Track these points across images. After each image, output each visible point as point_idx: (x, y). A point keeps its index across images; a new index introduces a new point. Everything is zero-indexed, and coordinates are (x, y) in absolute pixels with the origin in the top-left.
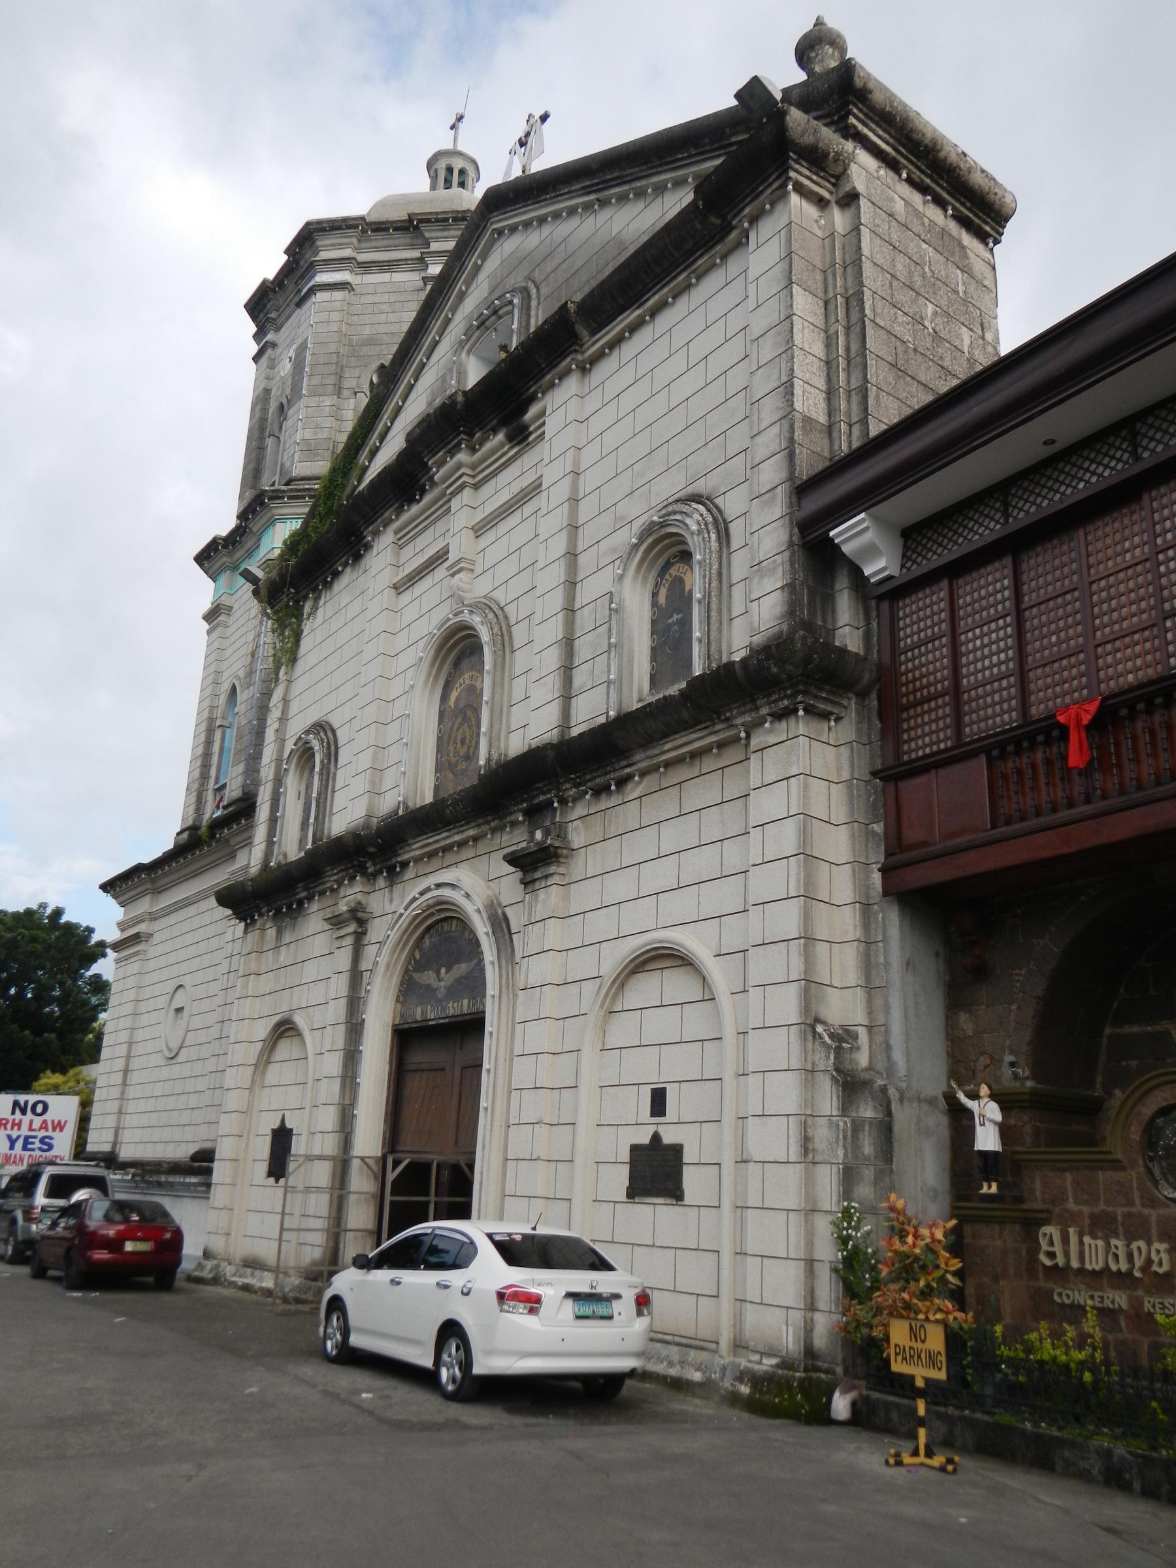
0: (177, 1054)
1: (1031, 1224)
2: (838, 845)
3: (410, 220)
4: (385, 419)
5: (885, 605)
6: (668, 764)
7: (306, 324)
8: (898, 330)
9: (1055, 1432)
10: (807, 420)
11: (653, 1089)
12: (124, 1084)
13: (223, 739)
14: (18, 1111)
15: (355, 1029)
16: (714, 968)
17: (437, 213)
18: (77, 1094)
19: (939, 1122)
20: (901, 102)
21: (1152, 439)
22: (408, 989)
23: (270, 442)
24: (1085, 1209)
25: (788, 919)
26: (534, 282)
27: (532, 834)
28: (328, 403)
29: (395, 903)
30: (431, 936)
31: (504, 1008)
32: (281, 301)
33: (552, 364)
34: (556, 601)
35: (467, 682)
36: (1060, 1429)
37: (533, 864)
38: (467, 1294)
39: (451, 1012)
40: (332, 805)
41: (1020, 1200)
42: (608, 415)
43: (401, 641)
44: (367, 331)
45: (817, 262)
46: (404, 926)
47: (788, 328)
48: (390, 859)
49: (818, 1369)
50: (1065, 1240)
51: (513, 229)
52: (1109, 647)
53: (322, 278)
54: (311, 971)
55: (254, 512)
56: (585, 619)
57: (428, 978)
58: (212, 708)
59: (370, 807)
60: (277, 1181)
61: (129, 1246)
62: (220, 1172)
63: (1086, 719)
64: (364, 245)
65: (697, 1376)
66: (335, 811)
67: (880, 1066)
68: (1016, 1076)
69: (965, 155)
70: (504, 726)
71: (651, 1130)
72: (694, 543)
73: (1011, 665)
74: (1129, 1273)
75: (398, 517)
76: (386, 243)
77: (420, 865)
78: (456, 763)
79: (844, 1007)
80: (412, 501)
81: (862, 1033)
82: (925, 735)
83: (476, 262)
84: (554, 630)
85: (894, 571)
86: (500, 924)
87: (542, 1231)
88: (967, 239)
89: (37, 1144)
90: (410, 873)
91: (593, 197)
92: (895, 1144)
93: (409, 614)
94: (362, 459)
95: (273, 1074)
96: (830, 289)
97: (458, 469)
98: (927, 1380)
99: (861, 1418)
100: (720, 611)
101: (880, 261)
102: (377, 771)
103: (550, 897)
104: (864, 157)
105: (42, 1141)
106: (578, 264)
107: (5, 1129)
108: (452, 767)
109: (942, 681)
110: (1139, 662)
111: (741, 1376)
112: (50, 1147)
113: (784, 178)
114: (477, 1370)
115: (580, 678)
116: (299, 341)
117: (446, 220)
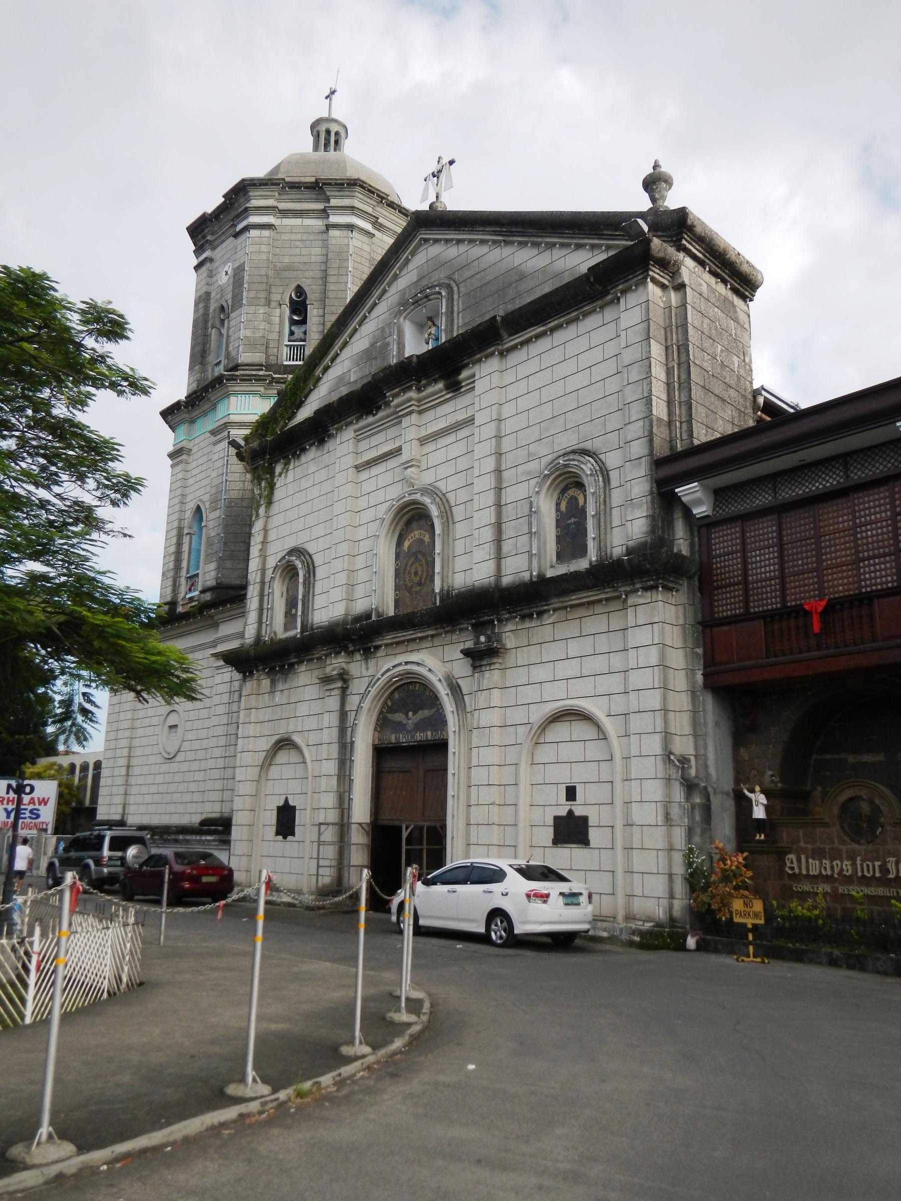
0: (175, 756)
1: (781, 854)
2: (678, 659)
3: (317, 182)
4: (336, 348)
5: (704, 531)
6: (572, 606)
7: (243, 252)
8: (705, 365)
9: (804, 947)
10: (659, 419)
11: (567, 787)
12: (128, 775)
13: (190, 543)
14: (11, 792)
15: (345, 748)
16: (608, 724)
17: (336, 179)
18: (52, 778)
19: (730, 804)
20: (711, 230)
21: (855, 468)
22: (383, 723)
23: (214, 333)
24: (810, 847)
25: (654, 700)
26: (454, 281)
27: (478, 638)
28: (261, 311)
29: (370, 670)
31: (462, 738)
32: (216, 228)
33: (481, 349)
34: (489, 499)
36: (806, 945)
38: (507, 894)
39: (419, 738)
41: (775, 842)
42: (521, 387)
43: (363, 503)
44: (287, 260)
45: (662, 324)
47: (647, 364)
49: (676, 927)
50: (799, 861)
51: (436, 241)
52: (830, 571)
53: (254, 219)
54: (302, 709)
55: (213, 387)
56: (509, 512)
57: (399, 717)
58: (180, 520)
59: (347, 609)
60: (285, 837)
61: (205, 879)
62: (236, 833)
63: (820, 609)
64: (282, 197)
65: (605, 934)
67: (702, 776)
68: (772, 781)
69: (739, 254)
70: (451, 570)
71: (569, 807)
72: (586, 481)
73: (777, 573)
74: (832, 876)
75: (357, 421)
76: (298, 196)
77: (389, 648)
78: (412, 587)
79: (683, 746)
80: (369, 412)
81: (692, 758)
82: (727, 604)
83: (407, 257)
84: (489, 516)
85: (709, 513)
86: (455, 690)
87: (531, 863)
88: (737, 301)
89: (28, 814)
90: (382, 652)
91: (500, 238)
92: (713, 816)
93: (369, 486)
94: (318, 372)
95: (274, 771)
96: (669, 340)
98: (753, 925)
99: (701, 947)
100: (605, 522)
101: (696, 324)
102: (351, 586)
103: (491, 676)
104: (689, 262)
105: (31, 812)
106: (489, 278)
107: (2, 804)
108: (409, 589)
109: (738, 576)
110: (845, 581)
111: (634, 932)
112: (38, 816)
113: (645, 274)
114: (516, 932)
115: (507, 547)
116: (237, 264)
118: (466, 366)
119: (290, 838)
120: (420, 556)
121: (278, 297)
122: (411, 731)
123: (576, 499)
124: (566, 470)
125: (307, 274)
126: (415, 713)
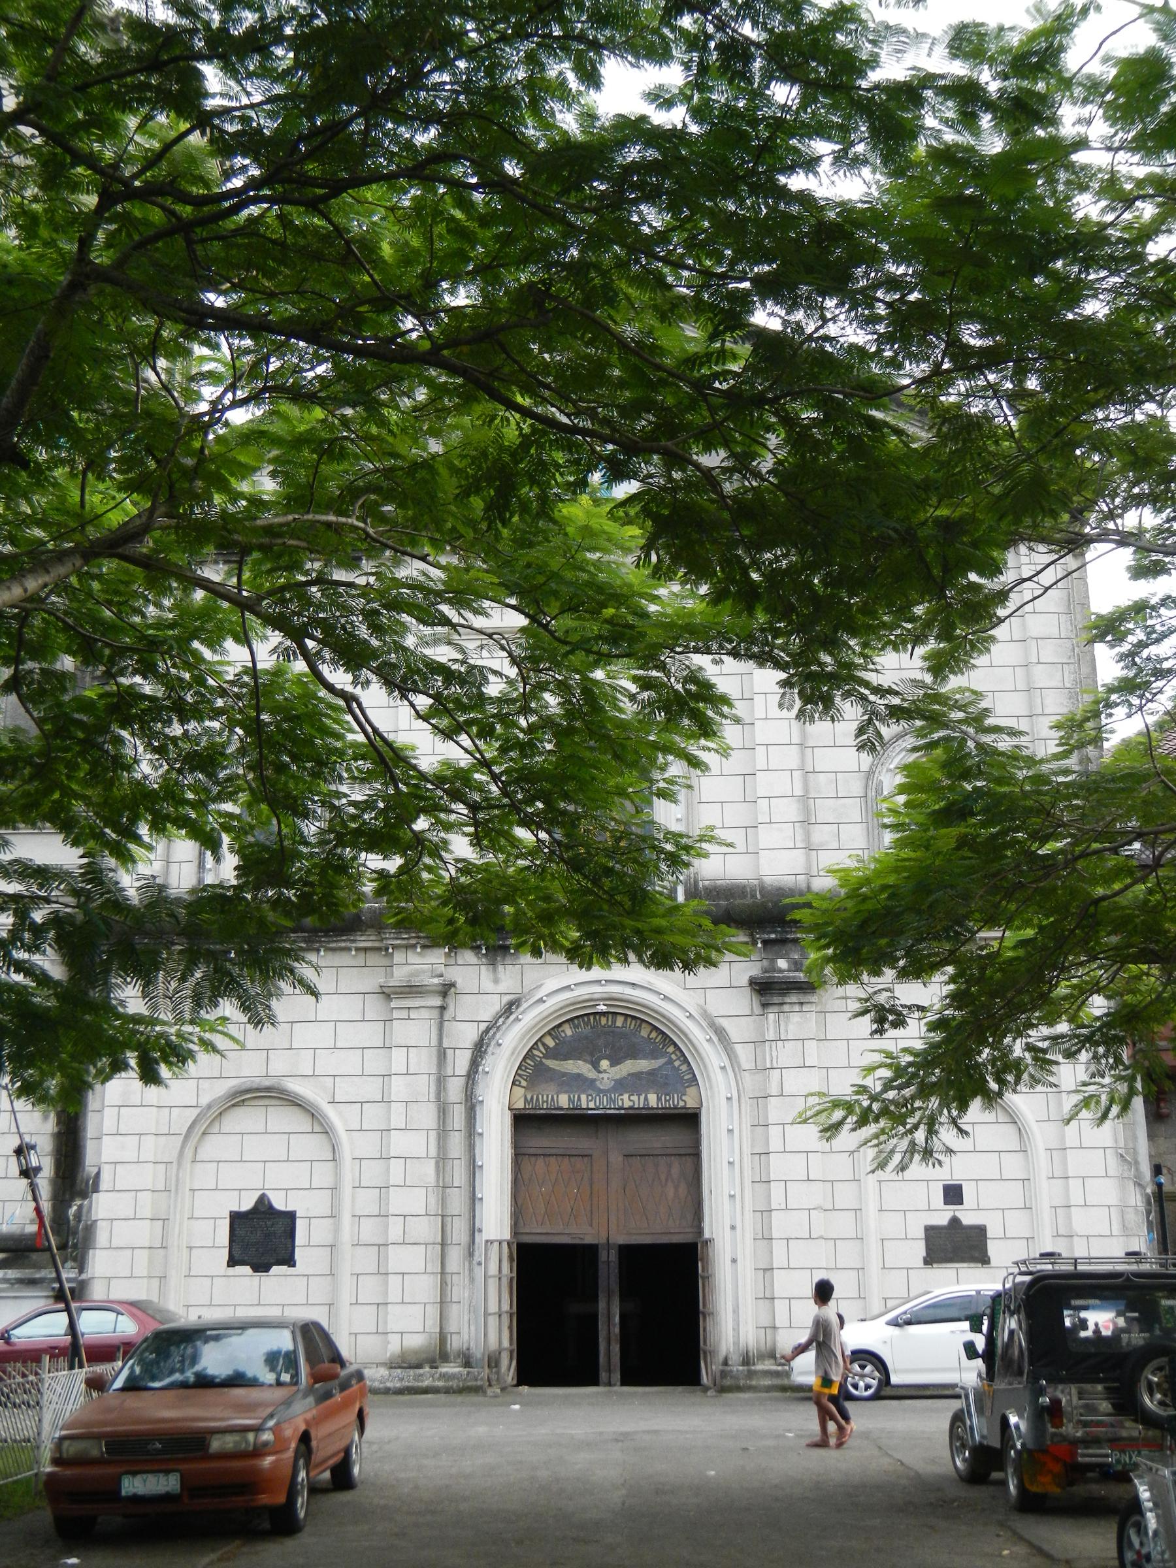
30: (576, 1027)
39: (627, 1104)
48: (505, 939)
95: (213, 1147)
119: (275, 1269)
122: (605, 1092)
126: (614, 1064)
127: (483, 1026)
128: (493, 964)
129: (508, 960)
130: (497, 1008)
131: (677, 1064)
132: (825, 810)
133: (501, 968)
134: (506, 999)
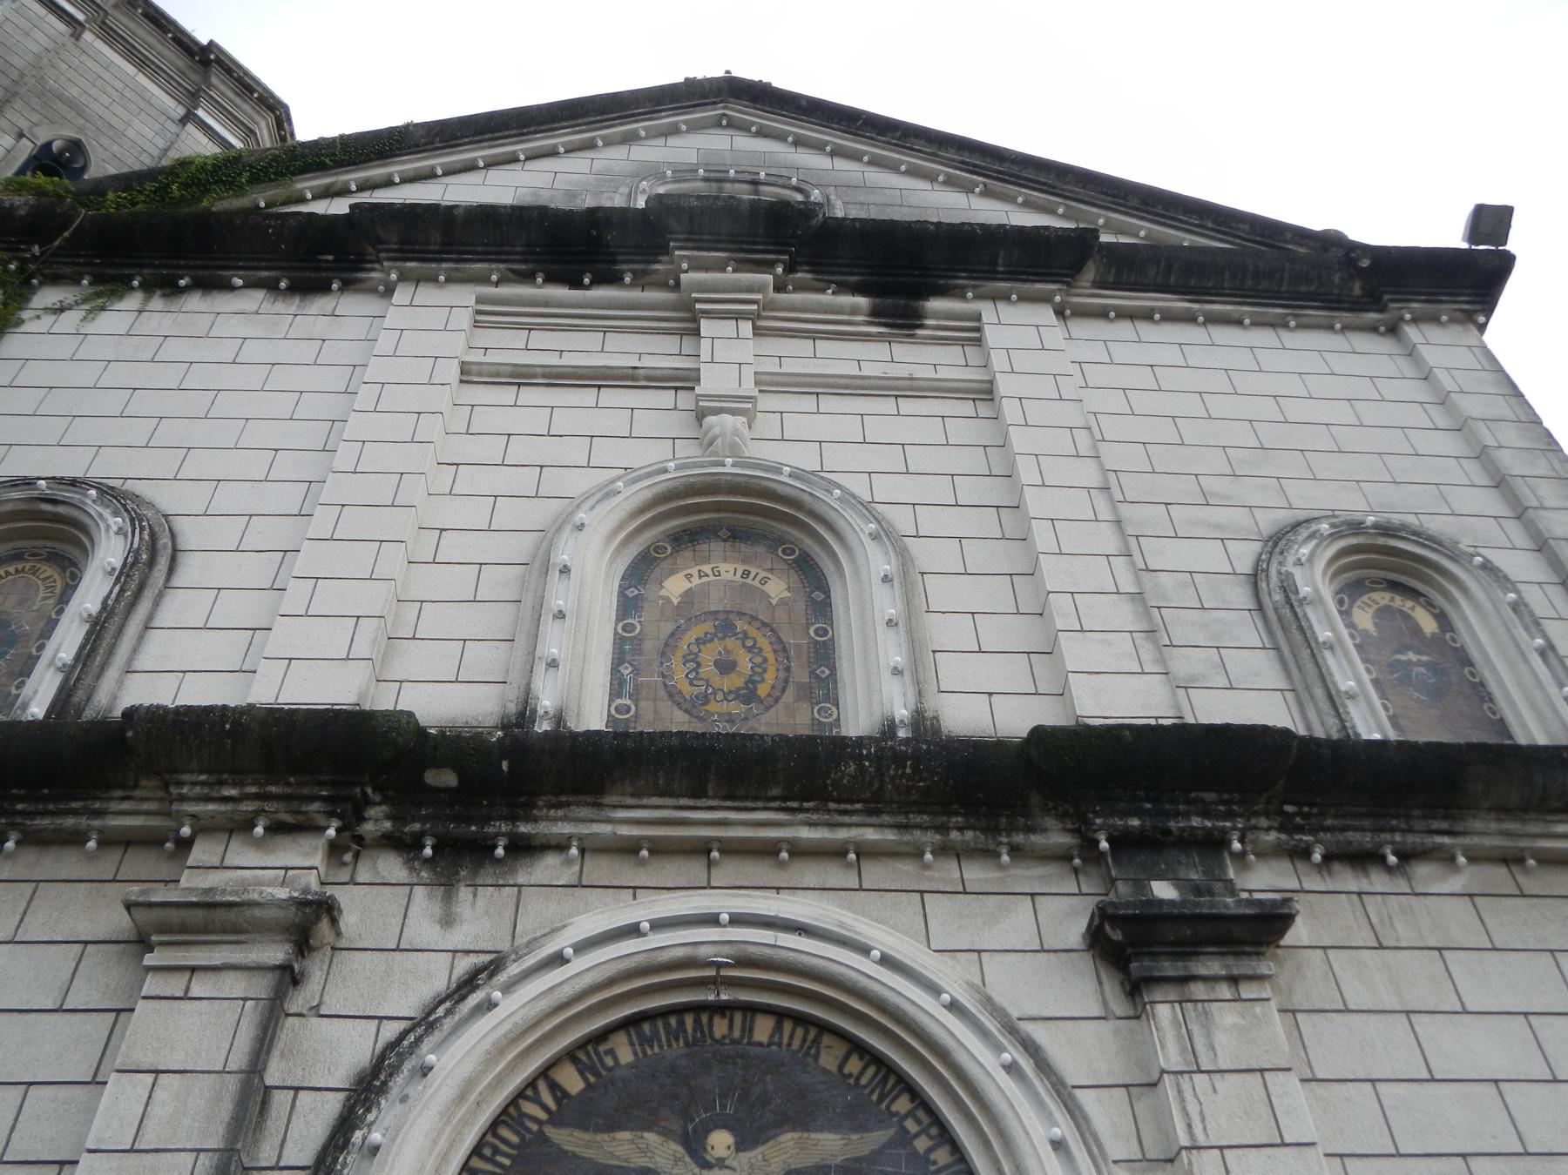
30: (646, 1041)
33: (1013, 275)
35: (725, 576)
37: (1136, 952)
40: (135, 651)
44: (75, 92)
46: (567, 992)
48: (485, 820)
51: (762, 133)
66: (144, 661)
90: (548, 868)
97: (750, 290)
117: (251, 90)
118: (958, 293)
120: (741, 625)
121: (24, 124)
123: (1407, 617)
124: (1381, 541)
125: (106, 142)
127: (390, 1031)
128: (446, 883)
129: (487, 875)
130: (440, 984)
131: (921, 1144)
132: (1183, 627)
133: (464, 893)
134: (464, 965)
